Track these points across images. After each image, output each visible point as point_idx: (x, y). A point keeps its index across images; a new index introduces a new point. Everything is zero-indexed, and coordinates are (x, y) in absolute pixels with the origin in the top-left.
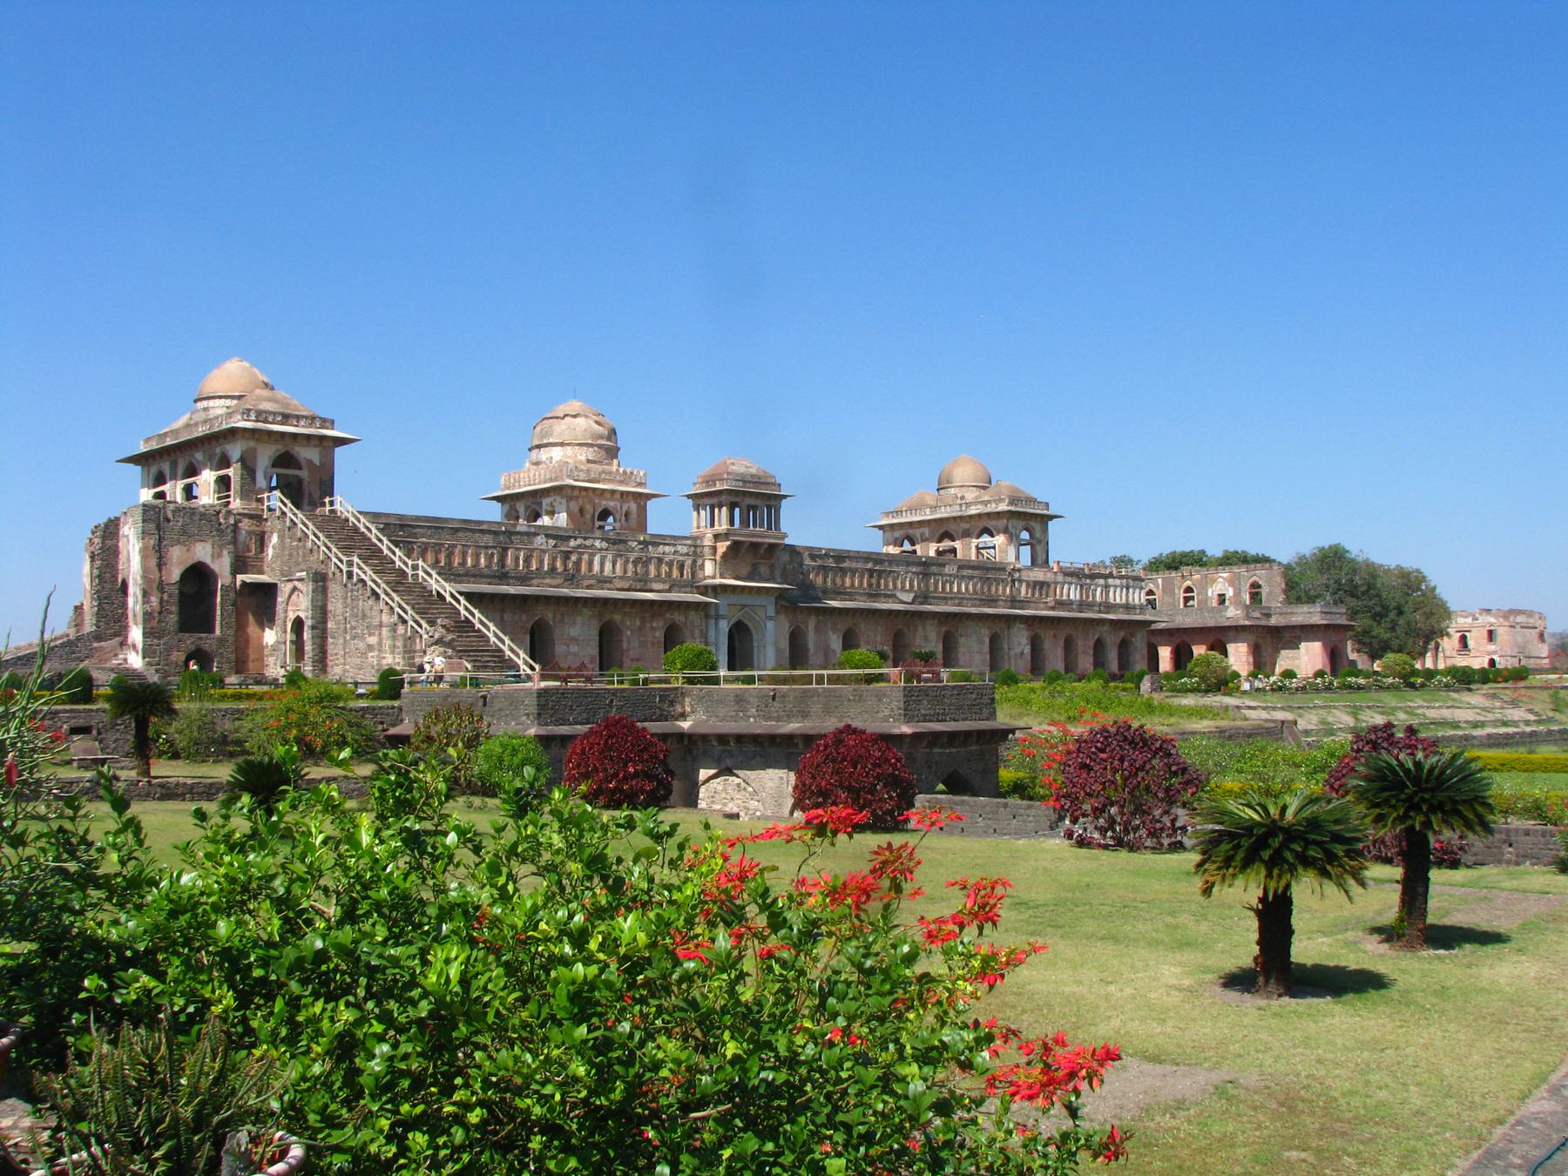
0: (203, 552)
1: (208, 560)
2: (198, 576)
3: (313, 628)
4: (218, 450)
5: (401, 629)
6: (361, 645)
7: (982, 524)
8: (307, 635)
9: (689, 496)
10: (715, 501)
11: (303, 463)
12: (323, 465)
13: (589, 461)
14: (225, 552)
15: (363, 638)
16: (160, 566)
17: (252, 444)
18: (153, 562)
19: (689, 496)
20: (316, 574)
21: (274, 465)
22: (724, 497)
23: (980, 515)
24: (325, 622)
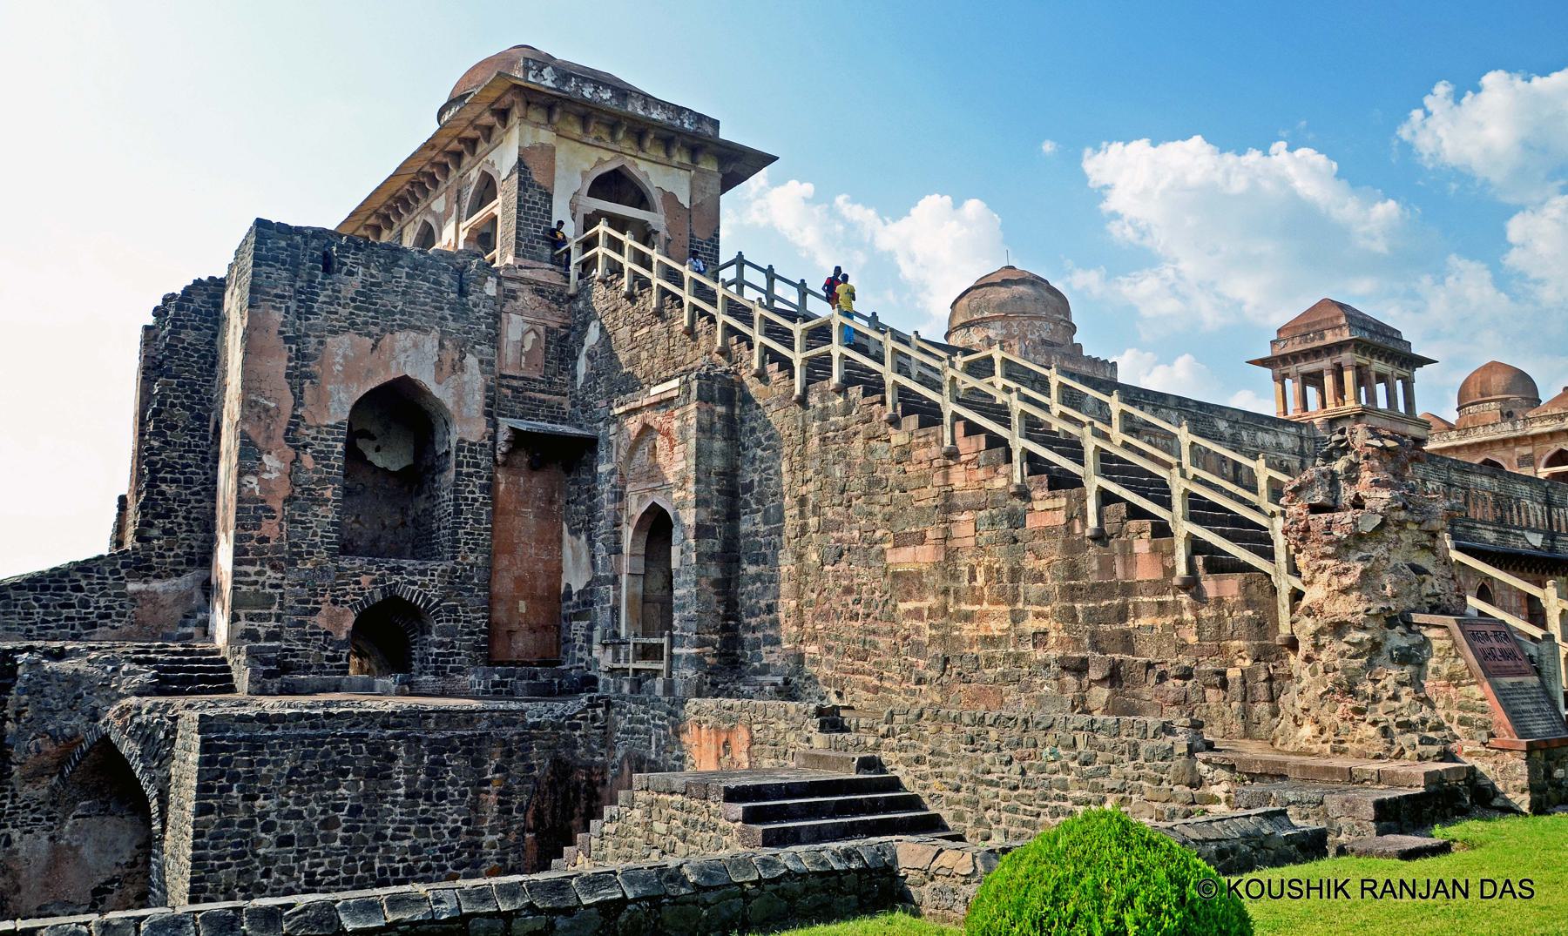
0: (413, 357)
1: (425, 377)
2: (399, 409)
3: (702, 531)
4: (474, 175)
5: (1047, 509)
6: (863, 576)
7: (1553, 448)
8: (682, 553)
9: (1263, 363)
10: (1325, 363)
11: (657, 198)
12: (696, 207)
13: (1044, 342)
14: (471, 361)
15: (869, 550)
16: (298, 377)
17: (545, 136)
18: (278, 364)
19: (1263, 363)
20: (707, 379)
21: (591, 193)
22: (1346, 357)
23: (1552, 435)
24: (732, 516)
